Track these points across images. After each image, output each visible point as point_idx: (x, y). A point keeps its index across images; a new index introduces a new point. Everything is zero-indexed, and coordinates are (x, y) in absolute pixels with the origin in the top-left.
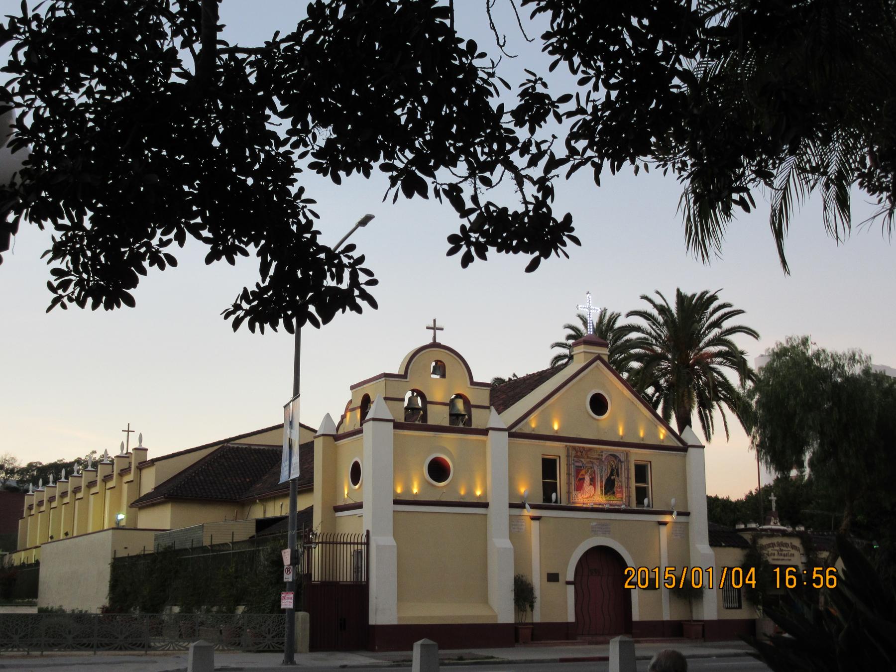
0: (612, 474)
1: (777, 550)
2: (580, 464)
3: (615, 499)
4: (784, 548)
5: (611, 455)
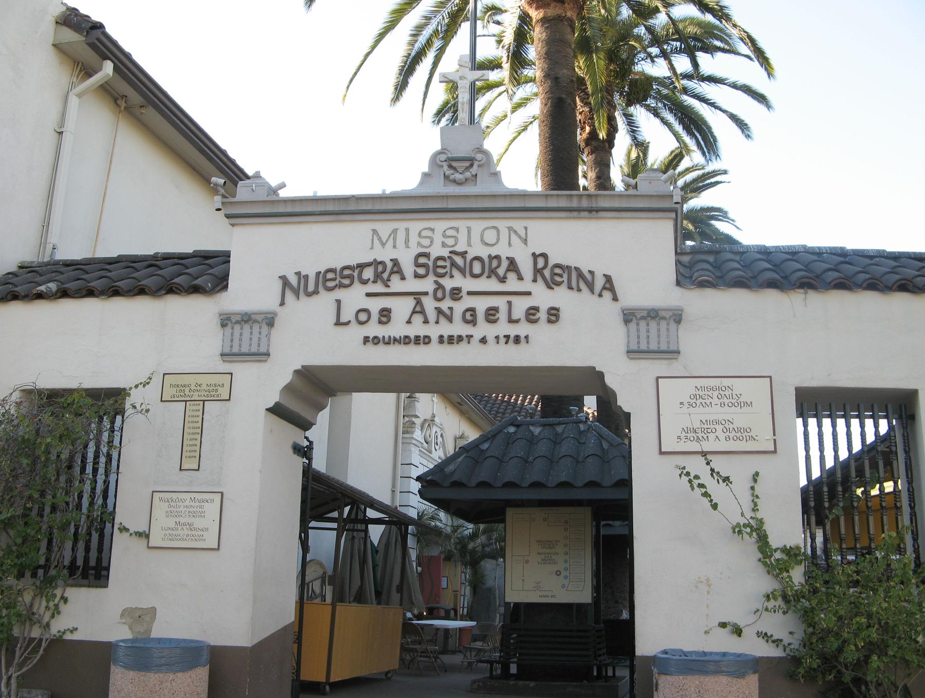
4: (468, 284)
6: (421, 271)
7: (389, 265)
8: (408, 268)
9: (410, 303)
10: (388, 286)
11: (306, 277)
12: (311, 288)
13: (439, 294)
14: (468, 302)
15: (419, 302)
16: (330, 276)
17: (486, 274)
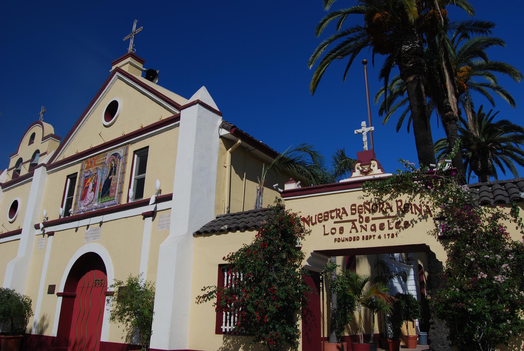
0: (110, 174)
1: (353, 221)
2: (87, 175)
3: (109, 199)
5: (113, 155)
6: (354, 212)
8: (349, 211)
15: (354, 224)
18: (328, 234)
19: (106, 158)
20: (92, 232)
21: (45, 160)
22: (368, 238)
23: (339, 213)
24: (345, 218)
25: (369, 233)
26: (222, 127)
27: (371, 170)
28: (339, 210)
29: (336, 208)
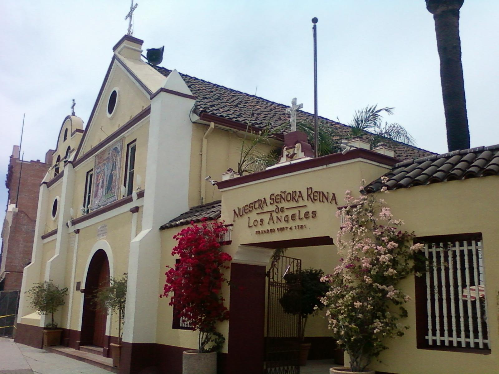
0: (112, 171)
4: (285, 205)
6: (272, 202)
7: (263, 200)
8: (268, 201)
9: (269, 215)
10: (263, 210)
11: (240, 209)
12: (241, 214)
13: (277, 211)
14: (287, 213)
15: (271, 214)
16: (247, 208)
17: (292, 199)
18: (251, 227)
19: (110, 153)
20: (102, 229)
21: (71, 158)
22: (282, 229)
23: (261, 203)
24: (266, 209)
25: (283, 225)
26: (195, 111)
27: (294, 154)
28: (261, 200)
29: (259, 199)
